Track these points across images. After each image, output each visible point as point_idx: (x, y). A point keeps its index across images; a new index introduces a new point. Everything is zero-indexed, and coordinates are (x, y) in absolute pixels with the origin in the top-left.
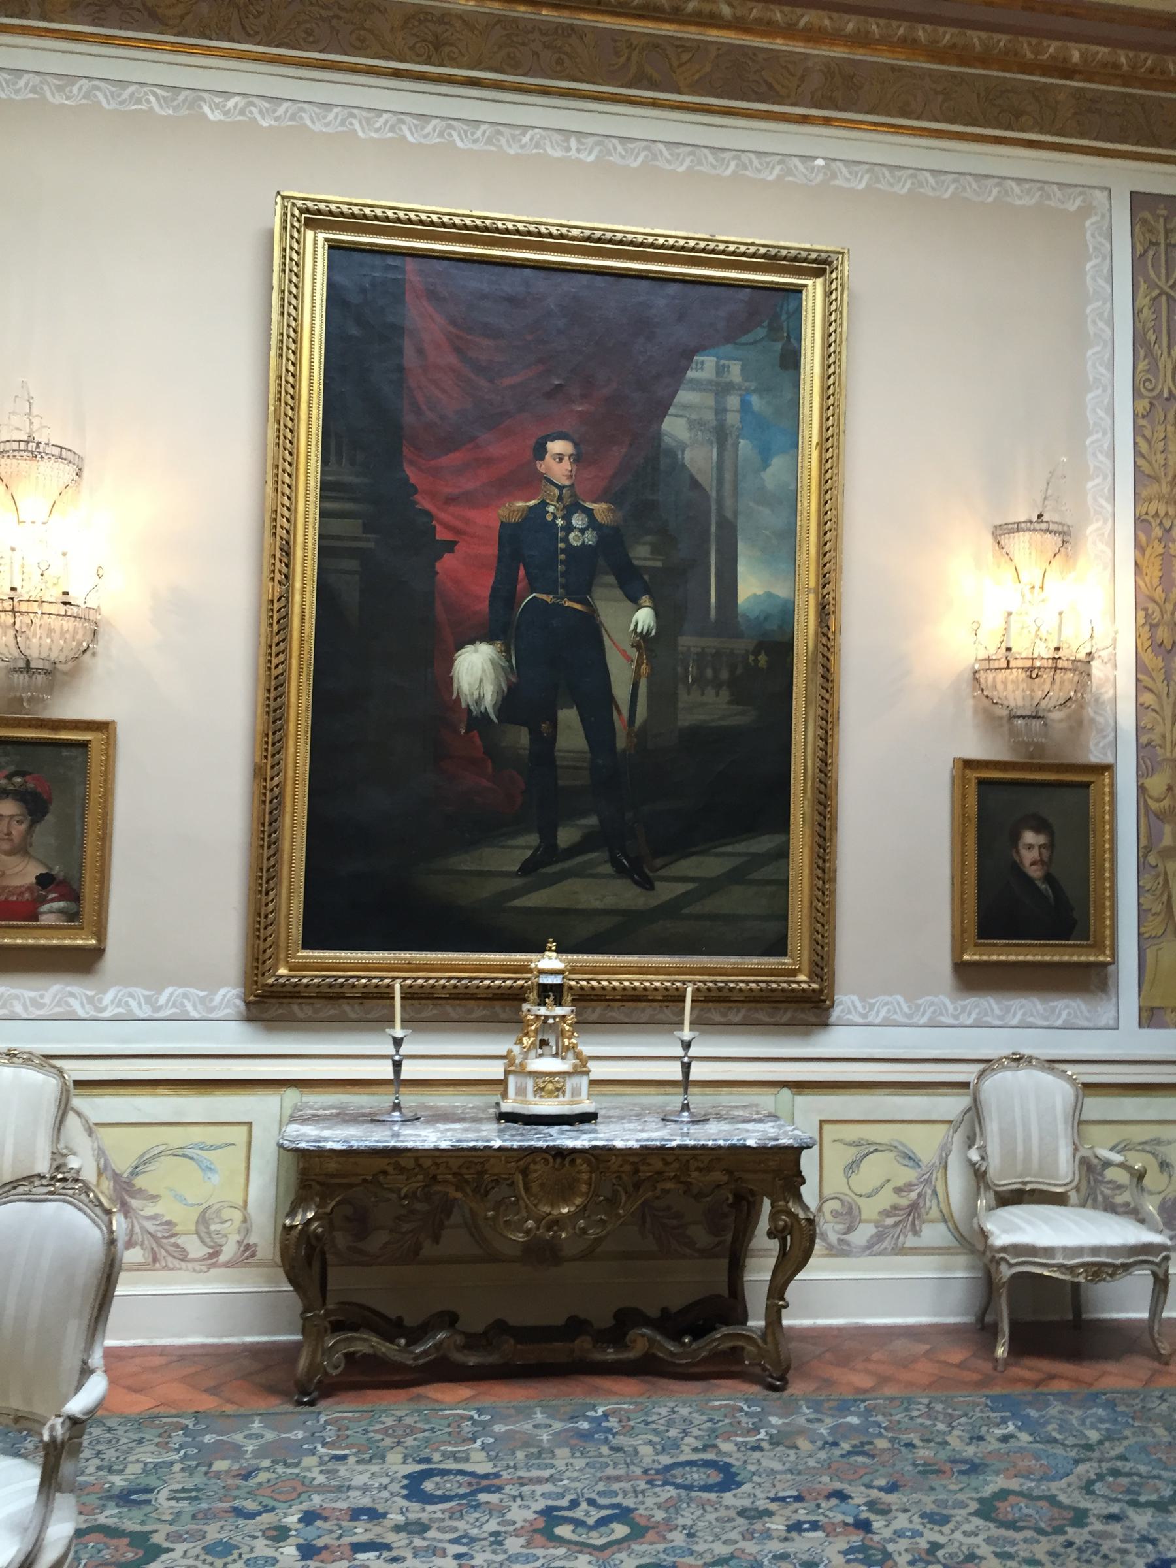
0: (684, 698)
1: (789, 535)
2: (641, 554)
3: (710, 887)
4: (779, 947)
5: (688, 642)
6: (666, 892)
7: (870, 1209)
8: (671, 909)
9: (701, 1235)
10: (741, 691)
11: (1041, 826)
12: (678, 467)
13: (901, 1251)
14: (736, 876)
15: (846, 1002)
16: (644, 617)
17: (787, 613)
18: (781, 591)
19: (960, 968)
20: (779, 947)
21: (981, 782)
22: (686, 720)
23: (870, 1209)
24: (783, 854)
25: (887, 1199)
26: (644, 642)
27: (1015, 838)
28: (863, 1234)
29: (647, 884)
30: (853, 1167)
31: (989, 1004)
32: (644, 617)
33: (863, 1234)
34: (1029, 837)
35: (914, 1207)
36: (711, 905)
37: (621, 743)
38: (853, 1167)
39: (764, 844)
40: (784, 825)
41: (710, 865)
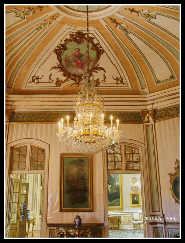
0: (113, 191)
1: (119, 180)
2: (110, 182)
3: (115, 202)
4: (120, 206)
5: (113, 187)
6: (113, 203)
7: (126, 222)
8: (113, 204)
9: (116, 224)
10: (116, 190)
11: (136, 197)
12: (112, 177)
13: (128, 224)
14: (117, 201)
15: (124, 209)
16: (110, 186)
17: (119, 185)
18: (119, 184)
19: (131, 206)
20: (120, 206)
21: (132, 195)
22: (113, 192)
23: (126, 222)
24: (120, 200)
25: (127, 221)
26: (110, 187)
27: (134, 198)
28: (126, 223)
29: (111, 202)
30: (125, 219)
31: (133, 209)
32: (110, 186)
33: (126, 223)
34: (135, 198)
35: (129, 222)
36: (116, 203)
37: (109, 193)
38: (125, 219)
39: (118, 199)
40: (119, 198)
41: (115, 201)
